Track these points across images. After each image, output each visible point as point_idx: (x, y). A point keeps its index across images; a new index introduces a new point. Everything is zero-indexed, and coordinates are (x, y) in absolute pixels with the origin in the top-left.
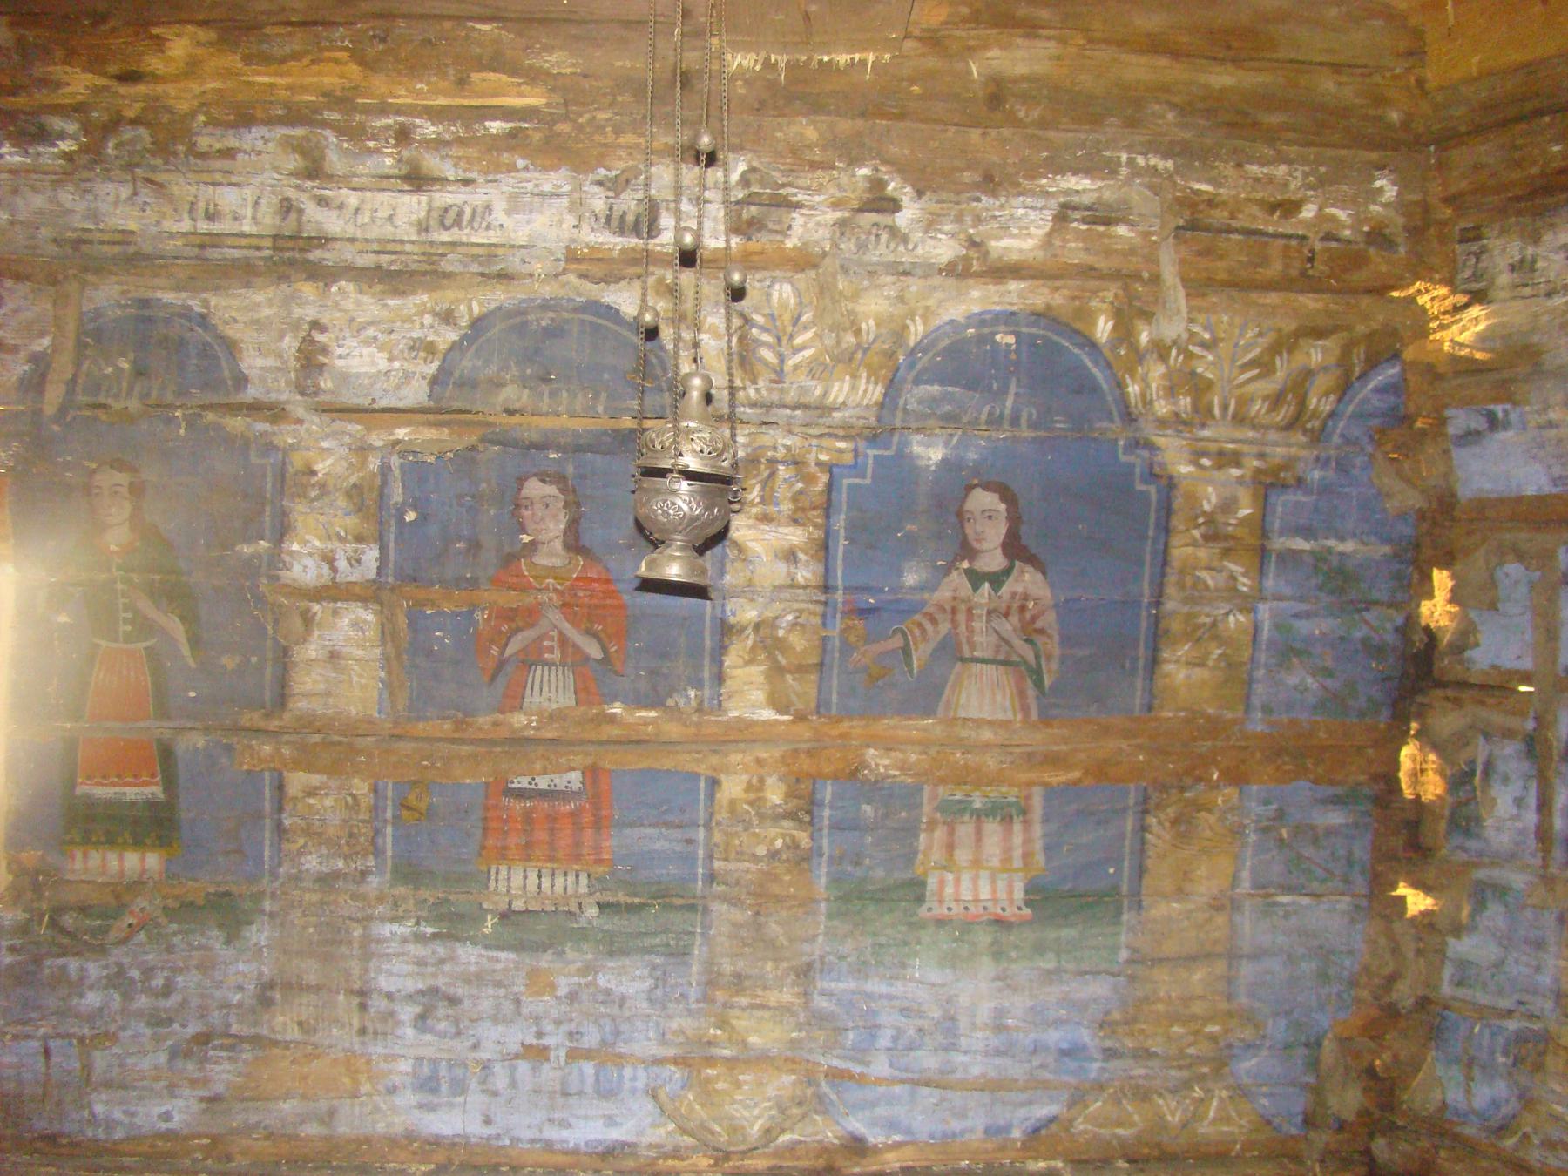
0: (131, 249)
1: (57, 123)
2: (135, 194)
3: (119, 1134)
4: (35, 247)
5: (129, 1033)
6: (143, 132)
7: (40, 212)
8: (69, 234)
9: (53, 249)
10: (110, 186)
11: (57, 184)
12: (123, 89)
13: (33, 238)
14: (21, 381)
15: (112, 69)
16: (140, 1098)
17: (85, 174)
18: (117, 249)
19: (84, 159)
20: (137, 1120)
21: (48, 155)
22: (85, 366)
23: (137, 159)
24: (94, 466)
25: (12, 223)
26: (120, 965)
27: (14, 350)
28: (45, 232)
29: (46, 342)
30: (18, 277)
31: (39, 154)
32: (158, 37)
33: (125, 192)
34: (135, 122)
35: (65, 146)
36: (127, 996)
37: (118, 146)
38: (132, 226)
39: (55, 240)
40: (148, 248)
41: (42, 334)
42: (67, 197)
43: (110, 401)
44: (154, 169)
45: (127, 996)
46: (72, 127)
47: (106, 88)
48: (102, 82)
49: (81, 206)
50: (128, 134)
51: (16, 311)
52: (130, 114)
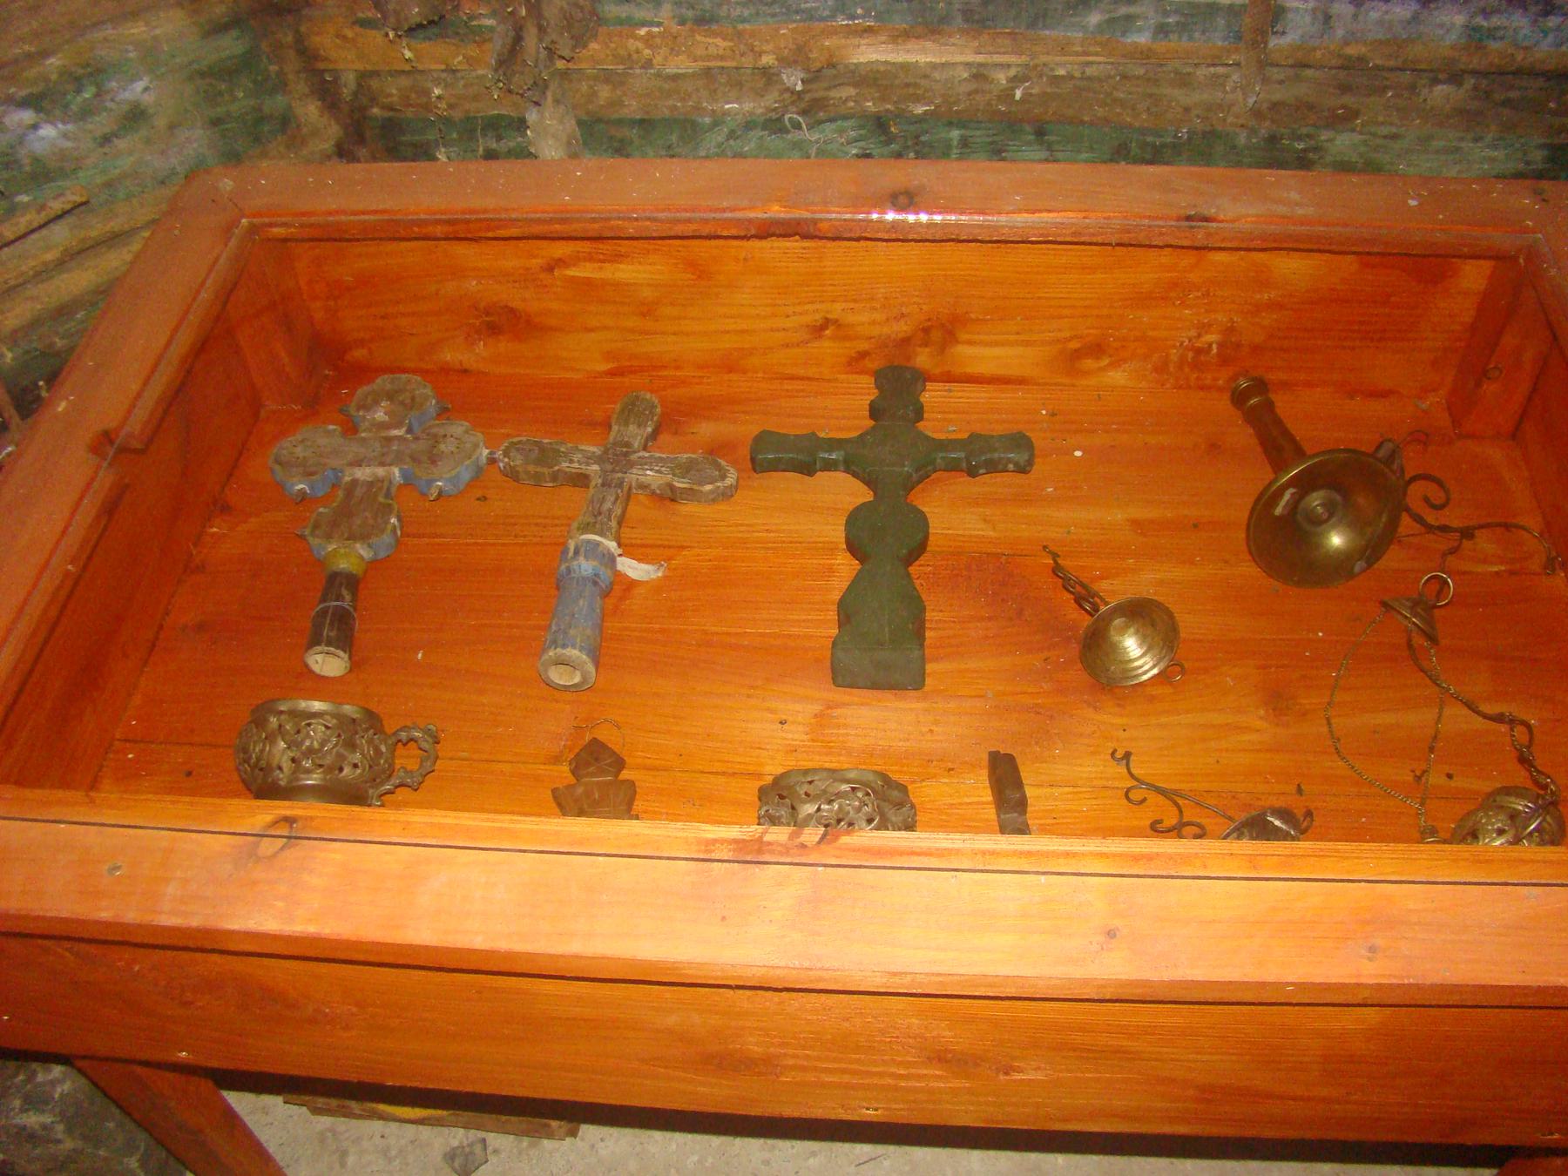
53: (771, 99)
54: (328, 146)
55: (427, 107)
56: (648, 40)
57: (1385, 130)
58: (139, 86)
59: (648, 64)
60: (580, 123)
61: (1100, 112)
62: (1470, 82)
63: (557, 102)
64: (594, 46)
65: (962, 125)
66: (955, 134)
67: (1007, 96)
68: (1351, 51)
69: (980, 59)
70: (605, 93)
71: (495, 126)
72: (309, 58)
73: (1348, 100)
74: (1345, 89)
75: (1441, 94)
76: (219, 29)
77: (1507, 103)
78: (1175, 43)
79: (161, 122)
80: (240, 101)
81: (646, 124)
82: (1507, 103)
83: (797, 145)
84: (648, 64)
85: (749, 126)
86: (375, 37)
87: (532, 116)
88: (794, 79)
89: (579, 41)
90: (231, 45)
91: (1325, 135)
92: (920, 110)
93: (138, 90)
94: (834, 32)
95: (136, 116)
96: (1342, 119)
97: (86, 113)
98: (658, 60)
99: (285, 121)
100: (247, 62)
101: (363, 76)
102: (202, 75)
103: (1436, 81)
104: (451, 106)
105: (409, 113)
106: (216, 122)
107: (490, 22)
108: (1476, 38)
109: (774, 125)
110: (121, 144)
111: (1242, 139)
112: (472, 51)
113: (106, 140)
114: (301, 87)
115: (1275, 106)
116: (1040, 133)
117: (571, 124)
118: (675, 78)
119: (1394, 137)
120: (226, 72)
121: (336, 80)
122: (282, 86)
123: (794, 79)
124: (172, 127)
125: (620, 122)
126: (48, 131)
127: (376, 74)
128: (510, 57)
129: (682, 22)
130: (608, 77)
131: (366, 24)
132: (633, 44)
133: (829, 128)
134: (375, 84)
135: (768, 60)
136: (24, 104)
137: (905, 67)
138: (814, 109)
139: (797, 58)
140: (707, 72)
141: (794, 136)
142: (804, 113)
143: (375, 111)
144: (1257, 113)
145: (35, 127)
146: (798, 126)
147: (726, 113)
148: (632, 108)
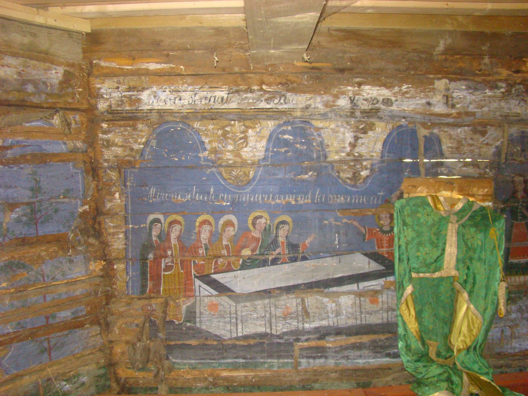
0: (520, 118)
1: (500, 84)
2: (519, 103)
3: (517, 350)
4: (496, 117)
5: (522, 323)
6: (521, 86)
7: (496, 108)
8: (504, 114)
9: (500, 118)
10: (513, 101)
11: (500, 100)
12: (515, 75)
13: (495, 115)
14: (494, 153)
15: (513, 70)
16: (524, 340)
17: (507, 98)
18: (516, 118)
19: (507, 94)
20: (522, 347)
21: (498, 92)
22: (509, 149)
23: (519, 94)
24: (514, 175)
25: (489, 111)
26: (520, 306)
27: (491, 145)
28: (498, 113)
29: (499, 143)
30: (491, 126)
31: (495, 93)
32: (524, 61)
33: (517, 102)
34: (519, 84)
35: (502, 90)
36: (522, 314)
37: (515, 90)
38: (519, 112)
39: (500, 116)
40: (524, 117)
41: (498, 141)
42: (503, 104)
43: (516, 158)
44: (524, 97)
45: (522, 314)
46: (504, 85)
47: (510, 75)
48: (511, 73)
49: (506, 106)
50: (517, 87)
51: (491, 134)
52: (518, 82)
53: (207, 383)
54: (116, 392)
55: (138, 385)
56: (183, 372)
57: (325, 383)
58: (85, 378)
59: (183, 376)
60: (169, 388)
61: (270, 383)
62: (338, 372)
63: (165, 384)
64: (173, 373)
65: (243, 387)
66: (242, 389)
67: (251, 381)
68: (315, 368)
69: (246, 374)
70: (174, 382)
71: (151, 389)
72: (115, 373)
73: (316, 377)
74: (315, 375)
75: (333, 375)
76: (101, 368)
77: (346, 376)
78: (282, 369)
79: (87, 385)
80: (102, 382)
81: (182, 389)
82: (346, 376)
83: (211, 392)
84: (183, 376)
85: (202, 388)
86: (130, 371)
87: (159, 387)
88: (211, 379)
89: (170, 372)
90: (102, 371)
91: (313, 384)
92: (235, 384)
93: (84, 379)
94: (218, 370)
95: (83, 384)
96: (315, 381)
97: (75, 383)
98: (185, 376)
99: (109, 387)
100: (105, 374)
101: (126, 378)
102: (96, 377)
103: (332, 373)
104: (143, 385)
105: (134, 386)
106: (97, 386)
107: (153, 368)
108: (337, 365)
109: (207, 388)
110: (79, 389)
111: (297, 386)
112: (149, 374)
113: (77, 388)
114: (113, 380)
115: (302, 380)
116: (259, 388)
117: (167, 388)
118: (188, 379)
119: (326, 384)
120: (100, 376)
121: (120, 379)
122: (110, 380)
123: (211, 379)
124: (89, 387)
125: (177, 388)
126: (67, 386)
127: (129, 378)
128: (156, 376)
129: (190, 369)
130: (174, 379)
131: (128, 368)
132: (180, 373)
133: (218, 388)
134: (128, 380)
135: (206, 375)
136: (65, 381)
137: (232, 376)
138: (215, 385)
139: (211, 375)
140: (194, 378)
141: (211, 390)
142: (213, 386)
143: (127, 385)
144: (299, 381)
145: (66, 385)
146: (212, 388)
147: (198, 386)
148: (179, 385)
